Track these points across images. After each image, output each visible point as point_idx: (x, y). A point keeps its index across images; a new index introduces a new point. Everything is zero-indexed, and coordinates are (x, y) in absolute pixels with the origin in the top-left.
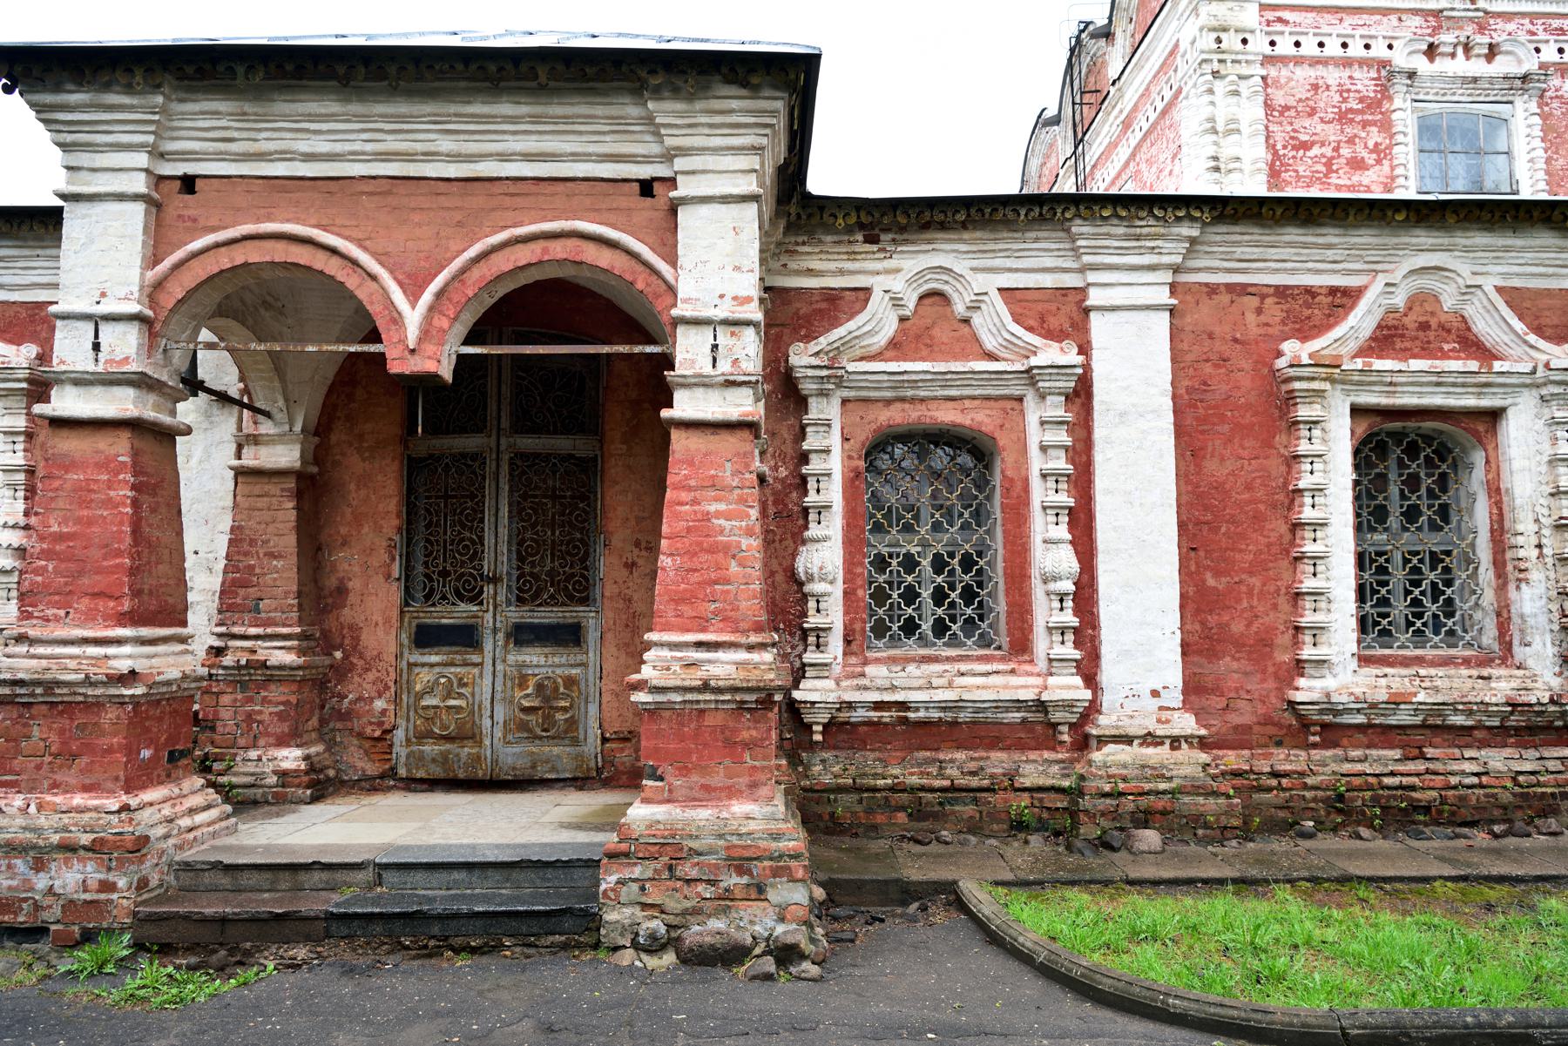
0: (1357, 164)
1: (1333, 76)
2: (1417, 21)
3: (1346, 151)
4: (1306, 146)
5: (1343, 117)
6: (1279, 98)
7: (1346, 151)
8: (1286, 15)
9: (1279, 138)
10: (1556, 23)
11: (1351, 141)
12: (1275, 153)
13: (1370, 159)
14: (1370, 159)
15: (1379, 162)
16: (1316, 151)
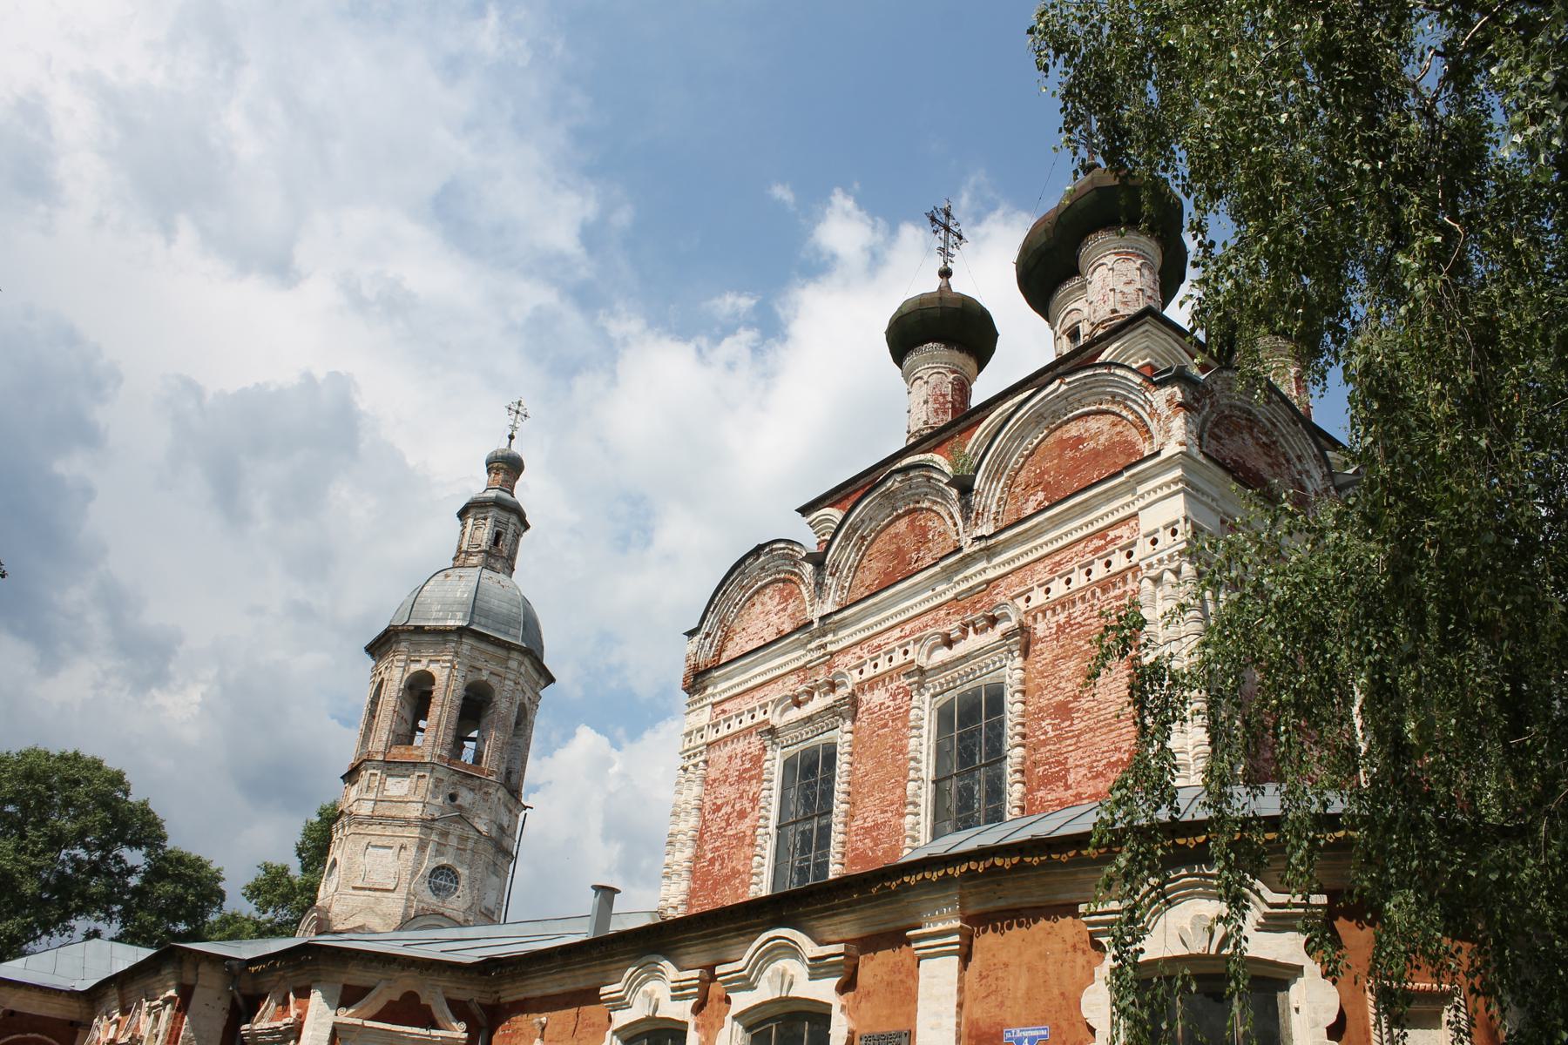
0: (742, 815)
1: (740, 746)
2: (794, 678)
3: (737, 807)
4: (718, 808)
5: (740, 779)
6: (713, 773)
7: (737, 807)
8: (726, 706)
9: (708, 805)
10: (875, 642)
11: (741, 797)
12: (704, 821)
13: (748, 805)
14: (748, 805)
15: (753, 809)
16: (723, 811)
